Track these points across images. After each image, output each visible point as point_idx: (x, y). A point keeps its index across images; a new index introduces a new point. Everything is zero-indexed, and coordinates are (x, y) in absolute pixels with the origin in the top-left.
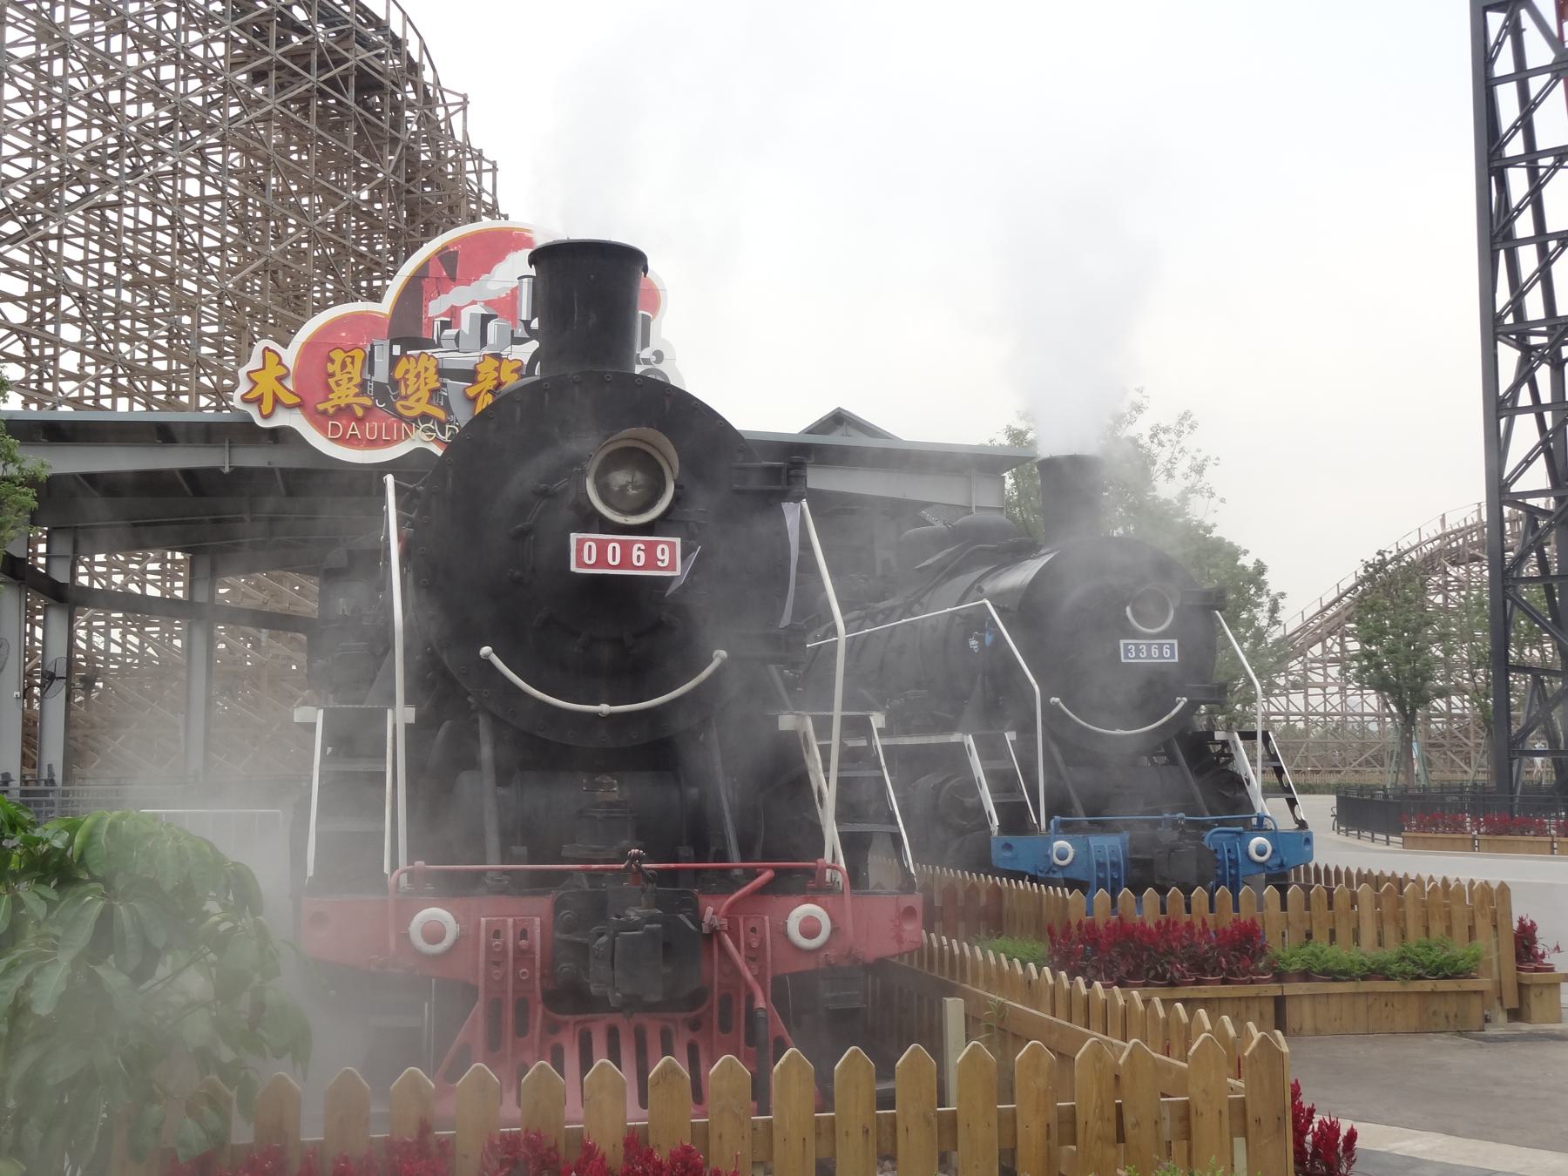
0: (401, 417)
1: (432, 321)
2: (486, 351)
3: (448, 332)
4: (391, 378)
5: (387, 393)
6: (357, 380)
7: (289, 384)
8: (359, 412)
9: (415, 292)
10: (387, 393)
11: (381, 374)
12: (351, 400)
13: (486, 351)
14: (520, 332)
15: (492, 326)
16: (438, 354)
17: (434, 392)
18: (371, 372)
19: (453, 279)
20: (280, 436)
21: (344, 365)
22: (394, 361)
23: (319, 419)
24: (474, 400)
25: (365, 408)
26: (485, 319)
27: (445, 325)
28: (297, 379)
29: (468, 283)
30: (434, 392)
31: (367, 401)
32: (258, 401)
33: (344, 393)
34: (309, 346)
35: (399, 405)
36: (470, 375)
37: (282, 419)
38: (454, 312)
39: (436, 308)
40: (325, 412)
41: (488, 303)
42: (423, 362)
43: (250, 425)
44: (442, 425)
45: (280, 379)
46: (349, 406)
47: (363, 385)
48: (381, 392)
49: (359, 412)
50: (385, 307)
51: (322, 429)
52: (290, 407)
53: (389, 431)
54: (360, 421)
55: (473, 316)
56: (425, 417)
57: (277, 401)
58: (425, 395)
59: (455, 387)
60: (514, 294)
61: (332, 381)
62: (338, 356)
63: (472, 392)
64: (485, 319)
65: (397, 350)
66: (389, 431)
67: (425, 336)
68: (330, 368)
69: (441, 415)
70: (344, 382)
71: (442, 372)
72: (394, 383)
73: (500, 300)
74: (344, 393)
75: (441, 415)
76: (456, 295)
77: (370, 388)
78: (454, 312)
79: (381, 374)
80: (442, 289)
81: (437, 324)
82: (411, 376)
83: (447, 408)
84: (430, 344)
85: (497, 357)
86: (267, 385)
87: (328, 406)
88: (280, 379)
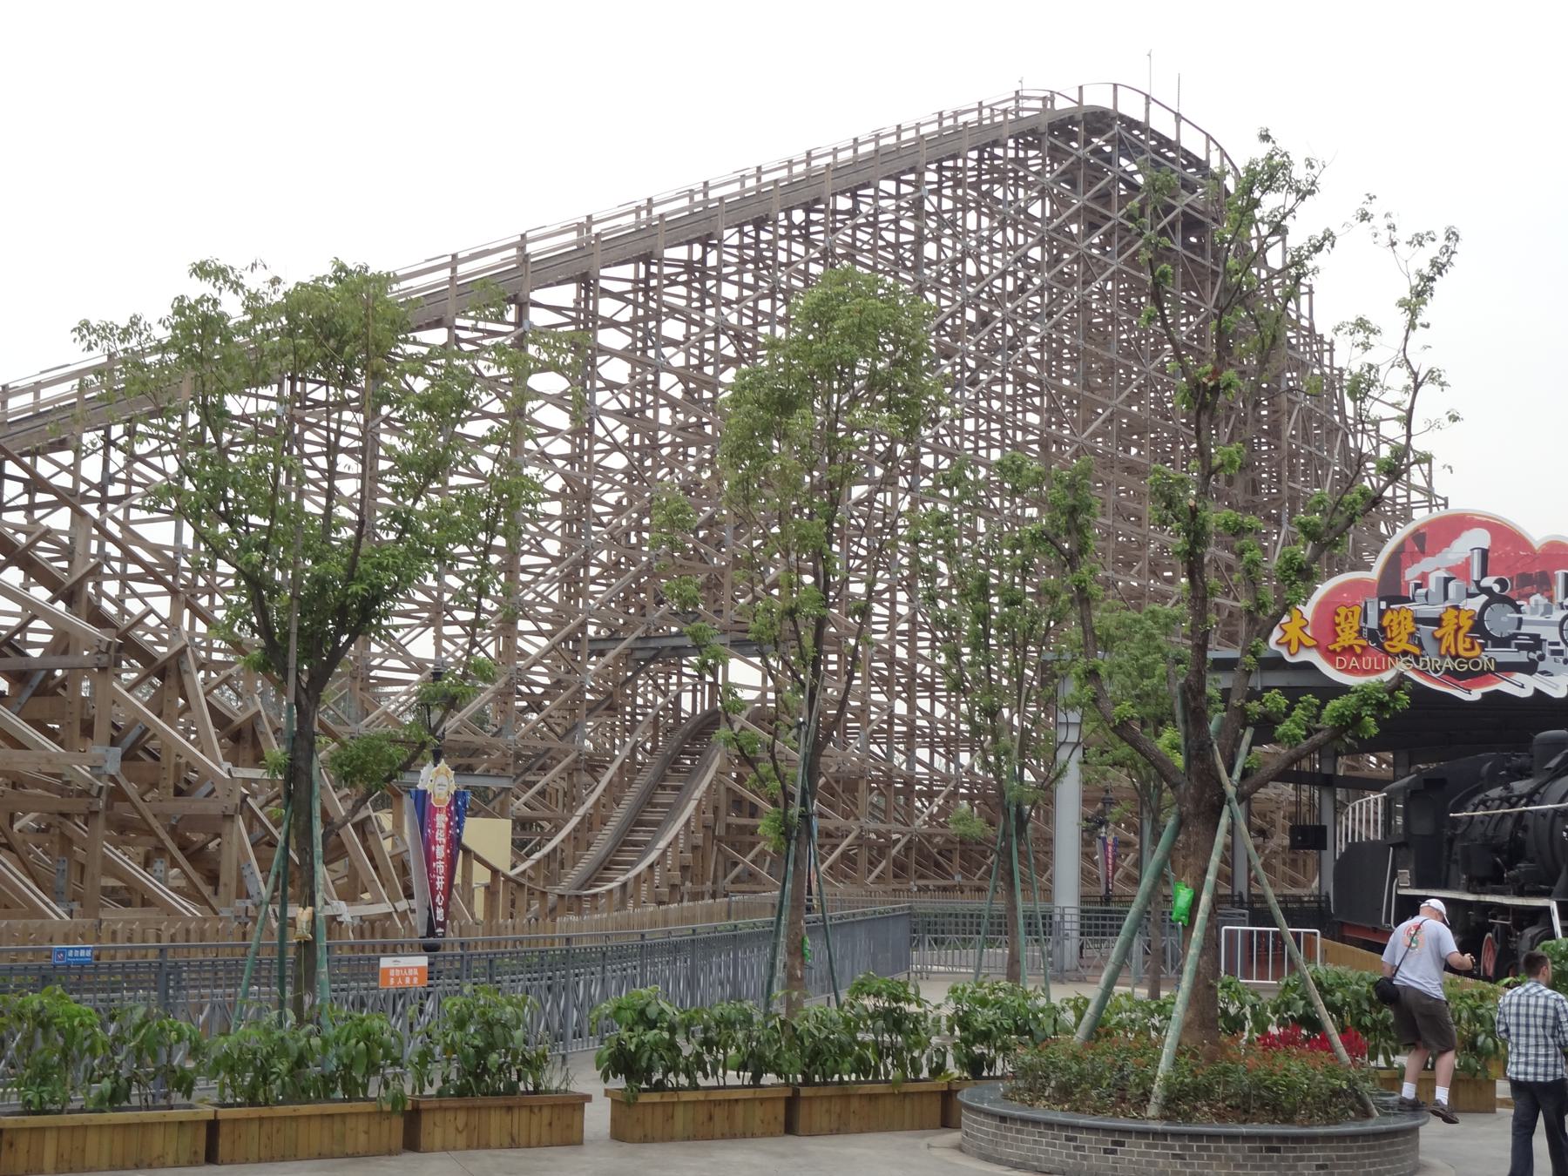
0: (1388, 653)
1: (1408, 583)
2: (1448, 604)
3: (1420, 591)
4: (1380, 625)
5: (1378, 636)
6: (1356, 628)
7: (1308, 631)
8: (1358, 650)
9: (1395, 564)
10: (1378, 636)
11: (1373, 623)
12: (1353, 642)
13: (1448, 604)
14: (1473, 589)
15: (1452, 585)
16: (1412, 606)
17: (1412, 635)
18: (1366, 621)
19: (1423, 553)
20: (1308, 666)
21: (1347, 617)
22: (1382, 613)
23: (1330, 655)
24: (1440, 640)
25: (1362, 647)
26: (1447, 581)
27: (1418, 586)
28: (1314, 628)
29: (1433, 554)
30: (1412, 635)
31: (1364, 643)
32: (1288, 644)
33: (1347, 637)
34: (1322, 605)
35: (1386, 645)
36: (1437, 622)
37: (1304, 656)
38: (1424, 577)
39: (1411, 574)
40: (1334, 651)
41: (1448, 569)
42: (1403, 612)
43: (1282, 659)
44: (1417, 658)
45: (1302, 628)
46: (1351, 647)
47: (1360, 632)
48: (1372, 635)
49: (1358, 650)
50: (1374, 575)
51: (1333, 663)
52: (1308, 647)
53: (1380, 663)
54: (1359, 657)
55: (1438, 579)
56: (1405, 653)
57: (1301, 643)
58: (1405, 637)
59: (1426, 630)
60: (1468, 562)
61: (1338, 629)
62: (1342, 611)
63: (1438, 635)
64: (1447, 581)
65: (1383, 605)
66: (1380, 663)
67: (1404, 594)
68: (1337, 620)
69: (1417, 651)
70: (1347, 630)
71: (1417, 620)
72: (1382, 629)
73: (1458, 567)
74: (1347, 637)
75: (1417, 651)
76: (1426, 564)
77: (1365, 633)
78: (1424, 577)
79: (1373, 623)
80: (1415, 559)
81: (1412, 586)
82: (1395, 624)
83: (1421, 646)
84: (1407, 600)
85: (1456, 608)
86: (1294, 633)
87: (1337, 647)
88: (1302, 628)
